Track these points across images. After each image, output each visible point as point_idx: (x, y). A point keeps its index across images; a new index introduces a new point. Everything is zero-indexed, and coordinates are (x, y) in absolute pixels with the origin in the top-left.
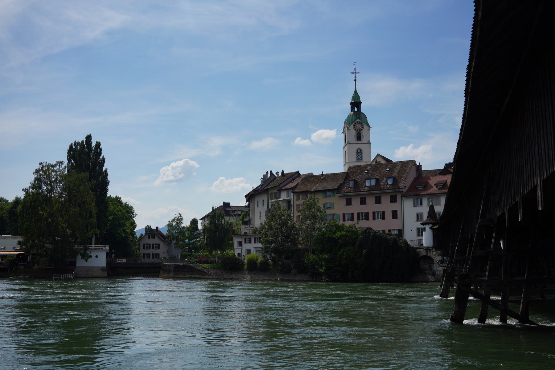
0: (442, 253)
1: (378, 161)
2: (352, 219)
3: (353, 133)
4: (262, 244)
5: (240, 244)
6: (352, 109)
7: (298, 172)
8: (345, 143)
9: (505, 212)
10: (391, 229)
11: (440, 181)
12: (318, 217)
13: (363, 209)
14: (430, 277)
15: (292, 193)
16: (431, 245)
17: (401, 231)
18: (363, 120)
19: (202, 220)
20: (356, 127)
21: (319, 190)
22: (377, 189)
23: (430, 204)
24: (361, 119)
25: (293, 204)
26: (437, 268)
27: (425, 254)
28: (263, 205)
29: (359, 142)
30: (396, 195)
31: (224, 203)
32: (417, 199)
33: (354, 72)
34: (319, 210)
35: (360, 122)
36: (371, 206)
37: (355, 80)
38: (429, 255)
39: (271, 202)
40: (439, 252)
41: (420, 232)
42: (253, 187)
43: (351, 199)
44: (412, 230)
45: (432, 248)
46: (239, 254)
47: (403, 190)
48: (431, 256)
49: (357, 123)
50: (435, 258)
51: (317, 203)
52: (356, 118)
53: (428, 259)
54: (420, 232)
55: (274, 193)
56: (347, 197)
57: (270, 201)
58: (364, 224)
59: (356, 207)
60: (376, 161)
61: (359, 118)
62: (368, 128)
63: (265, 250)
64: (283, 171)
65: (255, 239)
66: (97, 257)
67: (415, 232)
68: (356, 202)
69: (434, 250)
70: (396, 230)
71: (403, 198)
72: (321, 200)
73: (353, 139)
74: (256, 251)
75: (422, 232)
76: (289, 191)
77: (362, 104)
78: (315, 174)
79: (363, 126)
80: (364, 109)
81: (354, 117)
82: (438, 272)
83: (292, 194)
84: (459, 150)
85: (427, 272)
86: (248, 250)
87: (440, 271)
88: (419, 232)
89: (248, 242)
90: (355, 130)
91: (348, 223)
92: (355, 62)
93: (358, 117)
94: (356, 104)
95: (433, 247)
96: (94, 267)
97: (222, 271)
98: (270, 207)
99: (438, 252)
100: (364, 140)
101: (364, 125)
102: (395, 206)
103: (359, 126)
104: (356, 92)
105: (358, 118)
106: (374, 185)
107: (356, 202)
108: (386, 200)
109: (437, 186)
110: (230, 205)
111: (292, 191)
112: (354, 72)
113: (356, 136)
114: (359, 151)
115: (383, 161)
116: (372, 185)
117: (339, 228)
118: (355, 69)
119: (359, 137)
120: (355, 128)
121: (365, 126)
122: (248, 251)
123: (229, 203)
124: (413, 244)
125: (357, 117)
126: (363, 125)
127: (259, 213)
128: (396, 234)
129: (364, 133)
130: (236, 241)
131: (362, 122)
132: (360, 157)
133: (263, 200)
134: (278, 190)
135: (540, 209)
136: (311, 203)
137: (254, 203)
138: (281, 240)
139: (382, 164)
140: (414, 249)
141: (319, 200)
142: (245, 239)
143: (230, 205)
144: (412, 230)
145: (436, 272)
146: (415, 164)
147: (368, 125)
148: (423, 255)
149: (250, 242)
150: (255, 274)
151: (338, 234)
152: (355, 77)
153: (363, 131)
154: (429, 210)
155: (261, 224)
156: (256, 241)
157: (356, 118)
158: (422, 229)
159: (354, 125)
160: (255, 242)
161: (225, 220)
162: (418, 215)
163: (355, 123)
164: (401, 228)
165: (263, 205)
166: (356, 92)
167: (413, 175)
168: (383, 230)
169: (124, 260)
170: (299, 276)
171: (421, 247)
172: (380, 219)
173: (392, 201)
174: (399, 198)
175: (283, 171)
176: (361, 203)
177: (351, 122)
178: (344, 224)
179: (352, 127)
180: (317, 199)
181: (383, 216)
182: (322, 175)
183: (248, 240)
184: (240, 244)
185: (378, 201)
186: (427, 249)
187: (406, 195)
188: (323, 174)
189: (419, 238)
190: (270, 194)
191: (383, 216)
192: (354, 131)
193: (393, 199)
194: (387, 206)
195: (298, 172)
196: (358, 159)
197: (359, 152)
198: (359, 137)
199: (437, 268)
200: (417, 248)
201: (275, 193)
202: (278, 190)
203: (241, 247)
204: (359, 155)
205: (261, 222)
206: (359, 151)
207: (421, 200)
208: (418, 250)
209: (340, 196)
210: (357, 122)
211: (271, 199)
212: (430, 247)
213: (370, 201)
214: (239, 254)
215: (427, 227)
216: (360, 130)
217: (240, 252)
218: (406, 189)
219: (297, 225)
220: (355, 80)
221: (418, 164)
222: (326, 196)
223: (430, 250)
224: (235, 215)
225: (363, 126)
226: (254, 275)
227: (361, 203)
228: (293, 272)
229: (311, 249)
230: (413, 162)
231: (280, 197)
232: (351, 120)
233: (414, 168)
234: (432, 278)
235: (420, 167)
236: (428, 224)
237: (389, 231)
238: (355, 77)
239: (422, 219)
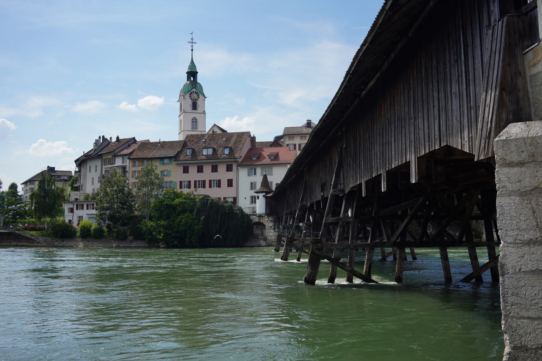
0: (273, 220)
1: (214, 131)
2: (189, 187)
3: (189, 102)
4: (96, 210)
5: (72, 210)
6: (188, 79)
7: (134, 138)
8: (181, 111)
9: (361, 184)
10: (226, 197)
11: (272, 153)
12: (156, 184)
13: (200, 177)
14: (262, 242)
15: (128, 159)
16: (264, 212)
17: (235, 199)
18: (199, 90)
19: (23, 185)
20: (192, 97)
21: (156, 157)
22: (213, 158)
23: (264, 174)
25: (128, 171)
26: (269, 233)
27: (258, 221)
28: (96, 171)
30: (232, 165)
31: (48, 167)
32: (251, 169)
34: (157, 177)
35: (196, 92)
36: (207, 175)
37: (192, 50)
38: (261, 221)
39: (105, 168)
40: (270, 218)
41: (253, 200)
42: (84, 152)
43: (188, 167)
44: (245, 198)
45: (264, 215)
46: (70, 221)
47: (238, 160)
48: (263, 222)
50: (267, 224)
51: (155, 170)
52: (192, 87)
53: (261, 225)
54: (253, 200)
55: (108, 159)
56: (213, 164)
57: (104, 167)
58: (201, 192)
59: (193, 175)
60: (213, 131)
61: (195, 88)
62: (204, 98)
63: (101, 216)
64: (118, 136)
65: (87, 205)
67: (249, 199)
68: (193, 170)
69: (266, 216)
70: (231, 197)
71: (238, 167)
72: (159, 168)
73: (189, 107)
74: (89, 217)
75: (255, 200)
76: (125, 157)
77: (198, 74)
78: (151, 141)
80: (200, 79)
81: (190, 86)
82: (269, 237)
83: (128, 160)
84: (319, 125)
85: (259, 237)
86: (80, 217)
87: (271, 236)
88: (252, 200)
89: (80, 209)
90: (191, 99)
91: (185, 191)
94: (192, 74)
95: (265, 214)
97: (52, 239)
98: (103, 173)
99: (269, 218)
100: (199, 109)
101: (200, 95)
102: (231, 175)
103: (195, 96)
104: (192, 62)
105: (194, 88)
106: (211, 154)
107: (193, 170)
108: (222, 168)
109: (269, 157)
110: (55, 170)
111: (128, 157)
112: (191, 41)
113: (192, 105)
114: (194, 121)
115: (219, 132)
116: (209, 154)
117: (177, 195)
118: (192, 39)
119: (195, 106)
120: (191, 98)
121: (201, 96)
122: (80, 218)
123: (54, 168)
124: (247, 211)
125: (193, 86)
126: (198, 95)
127: (92, 179)
128: (231, 202)
129: (199, 102)
130: (66, 207)
132: (195, 126)
133: (96, 166)
134: (113, 156)
135: (414, 182)
136: (149, 170)
137: (86, 168)
138: (117, 207)
139: (219, 134)
140: (248, 216)
141: (157, 167)
142: (77, 205)
143: (55, 170)
144: (245, 198)
145: (268, 237)
146: (250, 135)
147: (204, 95)
148: (256, 221)
149: (83, 209)
150: (88, 241)
151: (177, 201)
152: (192, 46)
153: (198, 101)
154: (263, 180)
155: (94, 190)
156: (89, 207)
157: (192, 87)
158: (255, 197)
159: (190, 95)
160: (87, 209)
161: (55, 185)
162: (252, 184)
163: (191, 93)
164: (236, 196)
165: (96, 171)
166: (192, 62)
167: (247, 146)
168: (218, 198)
170: (136, 243)
171: (254, 214)
172: (217, 187)
173: (228, 170)
174: (234, 167)
175: (118, 136)
176: (198, 172)
177: (187, 91)
178: (182, 192)
179: (187, 96)
180: (155, 166)
181: (219, 184)
182: (160, 143)
183: (80, 207)
184: (72, 210)
185: (215, 169)
186: (260, 216)
187: (241, 165)
188: (161, 141)
189: (253, 205)
190: (104, 159)
191: (219, 184)
192: (190, 100)
193: (229, 169)
194: (222, 174)
195: (134, 138)
196: (193, 128)
197: (194, 121)
198: (195, 106)
199: (269, 233)
200: (251, 215)
201: (110, 159)
202: (113, 156)
203: (72, 214)
204: (195, 124)
205: (94, 188)
207: (255, 170)
208: (252, 217)
209: (177, 164)
210: (193, 92)
211: (105, 165)
213: (207, 169)
214: (70, 221)
215: (261, 195)
216: (195, 100)
217: (71, 219)
218: (241, 159)
219: (134, 191)
220: (192, 50)
221: (252, 136)
222: (163, 164)
223: (262, 217)
224: (61, 180)
226: (88, 243)
227: (198, 172)
228: (129, 238)
229: (148, 216)
230: (249, 133)
231: (115, 163)
232: (187, 89)
233: (249, 140)
234: (264, 242)
235: (253, 139)
236: (262, 192)
237: (225, 198)
238: (192, 46)
239: (255, 188)
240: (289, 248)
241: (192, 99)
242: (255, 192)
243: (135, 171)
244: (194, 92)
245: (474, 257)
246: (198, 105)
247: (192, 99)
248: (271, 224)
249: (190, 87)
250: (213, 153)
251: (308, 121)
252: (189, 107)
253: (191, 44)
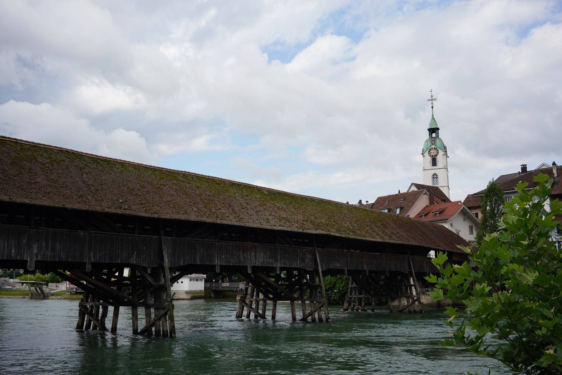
3: (429, 159)
6: (431, 134)
18: (438, 146)
24: (436, 145)
29: (435, 167)
35: (434, 148)
37: (432, 107)
49: (432, 149)
62: (443, 153)
66: (182, 282)
79: (437, 152)
81: (429, 143)
92: (432, 90)
93: (433, 143)
94: (433, 130)
96: (180, 291)
101: (439, 150)
104: (433, 118)
105: (433, 144)
112: (431, 99)
113: (431, 162)
114: (435, 176)
118: (432, 96)
120: (430, 154)
121: (441, 153)
125: (432, 142)
126: (438, 151)
129: (440, 158)
131: (437, 148)
152: (432, 104)
153: (438, 156)
157: (431, 144)
159: (429, 152)
163: (430, 150)
166: (433, 118)
169: (228, 284)
177: (426, 148)
179: (426, 154)
197: (435, 176)
206: (435, 176)
210: (432, 148)
216: (435, 156)
220: (432, 107)
225: (437, 152)
238: (432, 104)
240: (241, 306)
244: (433, 149)
245: (148, 315)
246: (438, 161)
249: (429, 144)
251: (523, 166)
252: (429, 164)
253: (431, 101)
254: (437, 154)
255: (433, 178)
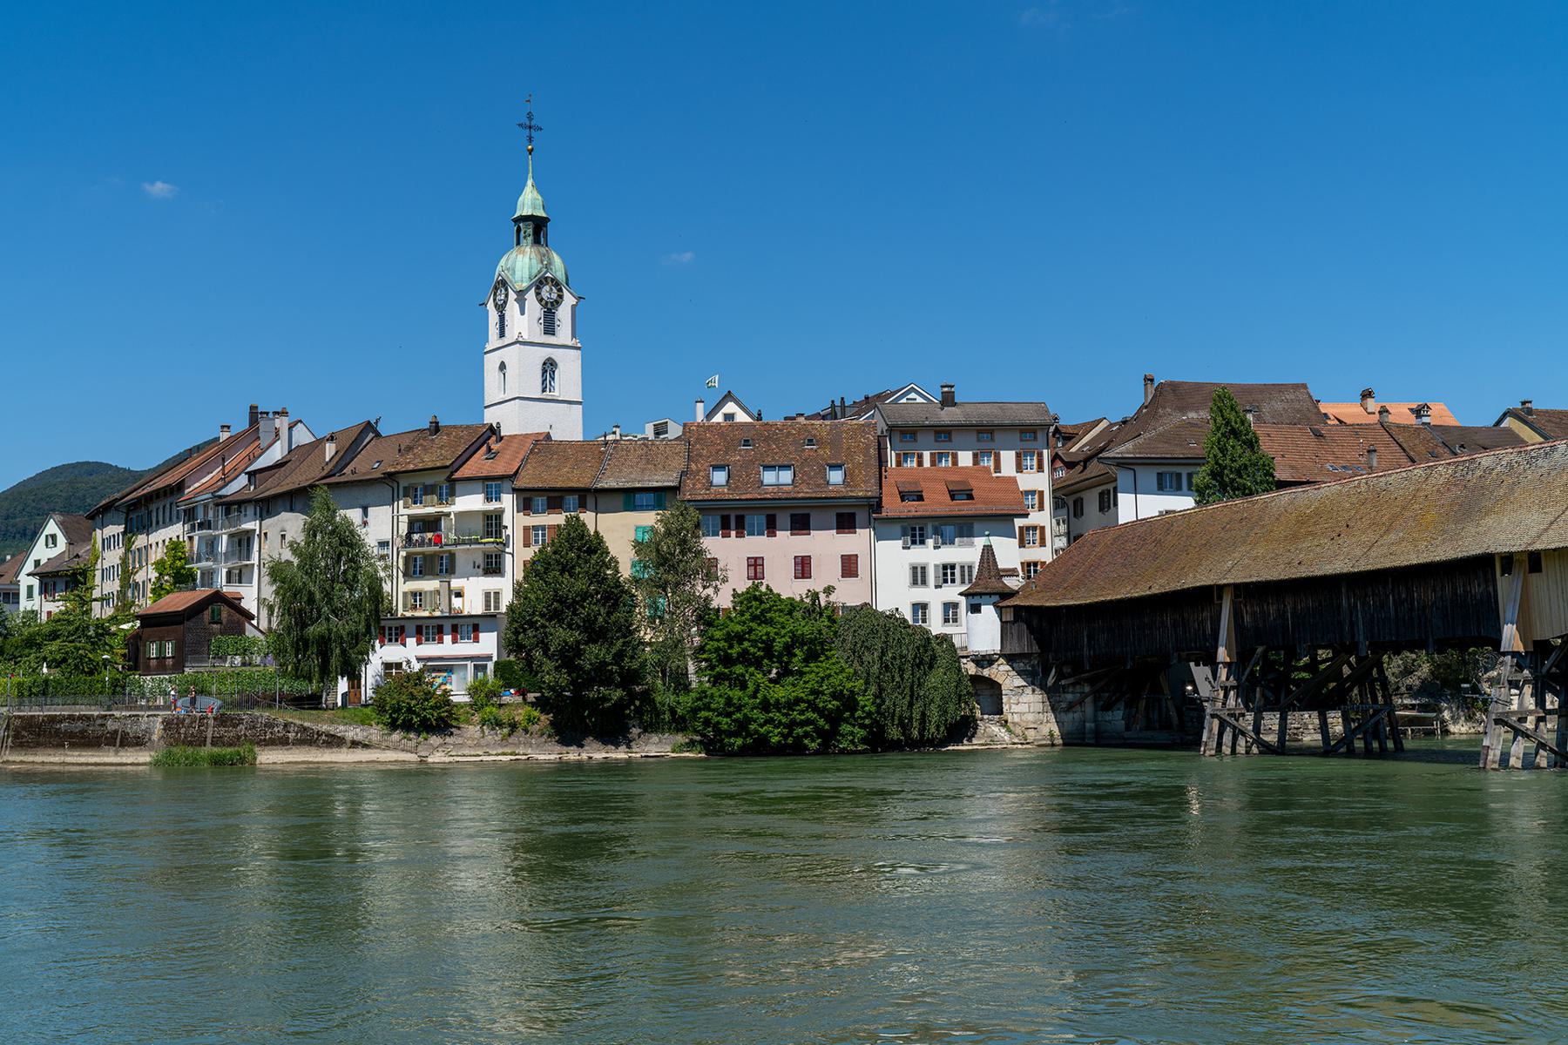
16: (998, 648)
26: (1013, 706)
33: (528, 123)
35: (552, 280)
48: (993, 677)
50: (1007, 681)
106: (790, 482)
118: (530, 116)
125: (542, 263)
152: (530, 140)
153: (560, 308)
162: (914, 569)
186: (984, 661)
190: (405, 488)
199: (1013, 706)
212: (995, 654)
234: (1003, 730)
236: (990, 594)
238: (530, 140)
241: (544, 302)
242: (961, 594)
243: (535, 528)
247: (544, 302)
248: (1019, 682)
250: (793, 481)
254: (559, 300)
255: (544, 372)
